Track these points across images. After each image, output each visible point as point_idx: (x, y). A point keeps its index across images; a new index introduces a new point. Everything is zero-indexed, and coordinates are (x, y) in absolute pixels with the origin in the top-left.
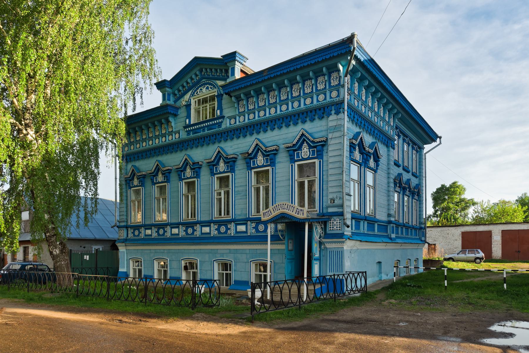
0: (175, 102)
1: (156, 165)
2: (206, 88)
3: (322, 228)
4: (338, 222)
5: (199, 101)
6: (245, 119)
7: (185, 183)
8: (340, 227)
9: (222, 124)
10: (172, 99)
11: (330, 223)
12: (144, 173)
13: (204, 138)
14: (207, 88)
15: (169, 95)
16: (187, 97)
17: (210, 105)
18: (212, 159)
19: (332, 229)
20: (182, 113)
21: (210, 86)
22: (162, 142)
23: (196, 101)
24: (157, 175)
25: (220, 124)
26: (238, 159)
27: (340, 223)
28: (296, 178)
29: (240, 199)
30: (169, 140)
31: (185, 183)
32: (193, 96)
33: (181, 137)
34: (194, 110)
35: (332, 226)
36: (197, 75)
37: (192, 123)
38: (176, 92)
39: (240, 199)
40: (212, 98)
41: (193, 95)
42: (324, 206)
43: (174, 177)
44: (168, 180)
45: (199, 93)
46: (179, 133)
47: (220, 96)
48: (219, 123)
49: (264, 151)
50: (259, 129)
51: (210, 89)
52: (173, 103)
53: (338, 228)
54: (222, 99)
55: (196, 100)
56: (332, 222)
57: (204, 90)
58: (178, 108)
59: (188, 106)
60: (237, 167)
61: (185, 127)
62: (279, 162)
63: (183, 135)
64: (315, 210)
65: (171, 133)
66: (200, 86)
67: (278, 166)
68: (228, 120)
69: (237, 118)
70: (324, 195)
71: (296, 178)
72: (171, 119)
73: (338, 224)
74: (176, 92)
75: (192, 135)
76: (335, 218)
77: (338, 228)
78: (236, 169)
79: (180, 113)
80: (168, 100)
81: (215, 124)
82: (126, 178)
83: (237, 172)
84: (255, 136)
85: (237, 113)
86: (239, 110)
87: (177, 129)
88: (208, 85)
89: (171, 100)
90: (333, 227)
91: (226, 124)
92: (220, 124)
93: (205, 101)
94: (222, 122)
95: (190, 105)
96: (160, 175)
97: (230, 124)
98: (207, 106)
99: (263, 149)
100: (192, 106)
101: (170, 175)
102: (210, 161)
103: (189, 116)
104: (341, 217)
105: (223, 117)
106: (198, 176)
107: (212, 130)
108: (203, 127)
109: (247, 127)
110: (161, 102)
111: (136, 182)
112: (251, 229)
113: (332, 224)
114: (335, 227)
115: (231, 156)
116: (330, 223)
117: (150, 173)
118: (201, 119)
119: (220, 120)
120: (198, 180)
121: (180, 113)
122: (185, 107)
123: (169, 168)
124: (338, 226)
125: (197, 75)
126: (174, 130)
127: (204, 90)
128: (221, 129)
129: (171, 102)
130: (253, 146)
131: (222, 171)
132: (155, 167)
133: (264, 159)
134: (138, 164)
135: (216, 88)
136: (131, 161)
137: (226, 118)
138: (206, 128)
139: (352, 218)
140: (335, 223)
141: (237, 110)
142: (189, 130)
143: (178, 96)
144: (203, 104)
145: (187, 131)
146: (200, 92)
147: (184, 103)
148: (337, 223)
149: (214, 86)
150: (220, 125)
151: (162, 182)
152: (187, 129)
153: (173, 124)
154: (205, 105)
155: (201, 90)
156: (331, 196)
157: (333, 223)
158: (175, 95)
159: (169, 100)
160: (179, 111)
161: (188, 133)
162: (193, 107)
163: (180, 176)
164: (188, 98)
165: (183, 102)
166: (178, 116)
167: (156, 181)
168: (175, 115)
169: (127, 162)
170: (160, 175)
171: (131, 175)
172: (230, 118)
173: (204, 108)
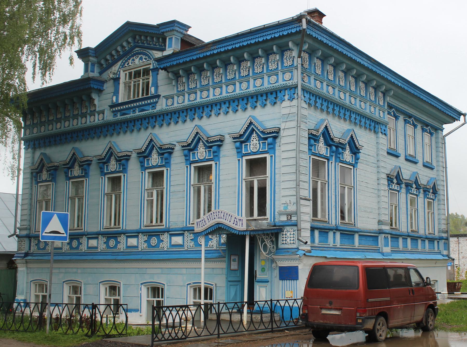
0: (101, 73)
1: (72, 153)
2: (139, 59)
3: (272, 241)
4: (292, 233)
5: (130, 74)
7: (109, 178)
9: (157, 105)
10: (97, 70)
11: (283, 235)
12: (56, 164)
13: (134, 121)
14: (141, 58)
15: (93, 65)
16: (115, 68)
17: (143, 80)
19: (284, 242)
20: (108, 87)
21: (144, 57)
22: (81, 124)
23: (126, 74)
24: (72, 167)
26: (175, 150)
27: (293, 234)
28: (244, 177)
30: (90, 122)
31: (109, 178)
32: (123, 67)
33: (105, 119)
34: (123, 85)
35: (284, 239)
36: (129, 43)
37: (120, 102)
38: (103, 62)
40: (146, 72)
41: (123, 66)
42: (276, 213)
43: (94, 171)
44: (86, 175)
45: (130, 64)
46: (103, 113)
47: (155, 70)
49: (205, 141)
51: (144, 60)
52: (98, 75)
54: (158, 74)
55: (127, 72)
56: (284, 233)
57: (137, 61)
58: (103, 82)
59: (116, 80)
60: (173, 161)
61: (111, 107)
62: (224, 156)
63: (109, 117)
64: (266, 217)
65: (93, 113)
66: (133, 56)
69: (176, 98)
70: (276, 199)
71: (244, 177)
72: (94, 96)
73: (292, 236)
74: (103, 62)
75: (119, 117)
76: (288, 228)
77: (292, 242)
79: (106, 88)
80: (91, 71)
81: (149, 104)
82: (32, 170)
83: (173, 167)
85: (175, 92)
87: (101, 109)
88: (141, 55)
89: (95, 71)
90: (286, 240)
91: (162, 105)
93: (137, 74)
94: (157, 102)
96: (77, 167)
97: (167, 105)
98: (139, 81)
101: (89, 168)
102: (140, 151)
103: (116, 93)
104: (295, 228)
105: (158, 96)
106: (124, 170)
107: (144, 112)
108: (135, 107)
109: (187, 109)
110: (83, 74)
111: (45, 175)
113: (284, 236)
114: (288, 240)
115: (167, 147)
116: (283, 235)
117: (64, 165)
118: (132, 96)
119: (155, 100)
120: (124, 175)
121: (106, 88)
122: (112, 81)
123: (89, 158)
124: (292, 239)
125: (129, 43)
126: (97, 110)
127: (137, 61)
128: (155, 111)
129: (95, 74)
131: (155, 164)
132: (70, 157)
134: (49, 151)
135: (151, 60)
136: (40, 147)
138: (137, 109)
139: (313, 229)
140: (288, 234)
141: (175, 88)
142: (116, 111)
143: (104, 66)
144: (135, 78)
145: (113, 112)
146: (132, 63)
147: (111, 76)
148: (290, 234)
149: (149, 57)
150: (154, 105)
151: (79, 177)
152: (114, 109)
153: (96, 102)
154: (137, 79)
155: (133, 60)
156: (284, 200)
157: (286, 234)
158: (102, 65)
159: (93, 71)
160: (105, 86)
162: (122, 80)
163: (101, 169)
164: (117, 70)
165: (110, 74)
166: (104, 92)
167: (71, 174)
168: (100, 91)
169: (34, 149)
170: (77, 167)
171: (39, 166)
172: (167, 98)
173: (136, 83)
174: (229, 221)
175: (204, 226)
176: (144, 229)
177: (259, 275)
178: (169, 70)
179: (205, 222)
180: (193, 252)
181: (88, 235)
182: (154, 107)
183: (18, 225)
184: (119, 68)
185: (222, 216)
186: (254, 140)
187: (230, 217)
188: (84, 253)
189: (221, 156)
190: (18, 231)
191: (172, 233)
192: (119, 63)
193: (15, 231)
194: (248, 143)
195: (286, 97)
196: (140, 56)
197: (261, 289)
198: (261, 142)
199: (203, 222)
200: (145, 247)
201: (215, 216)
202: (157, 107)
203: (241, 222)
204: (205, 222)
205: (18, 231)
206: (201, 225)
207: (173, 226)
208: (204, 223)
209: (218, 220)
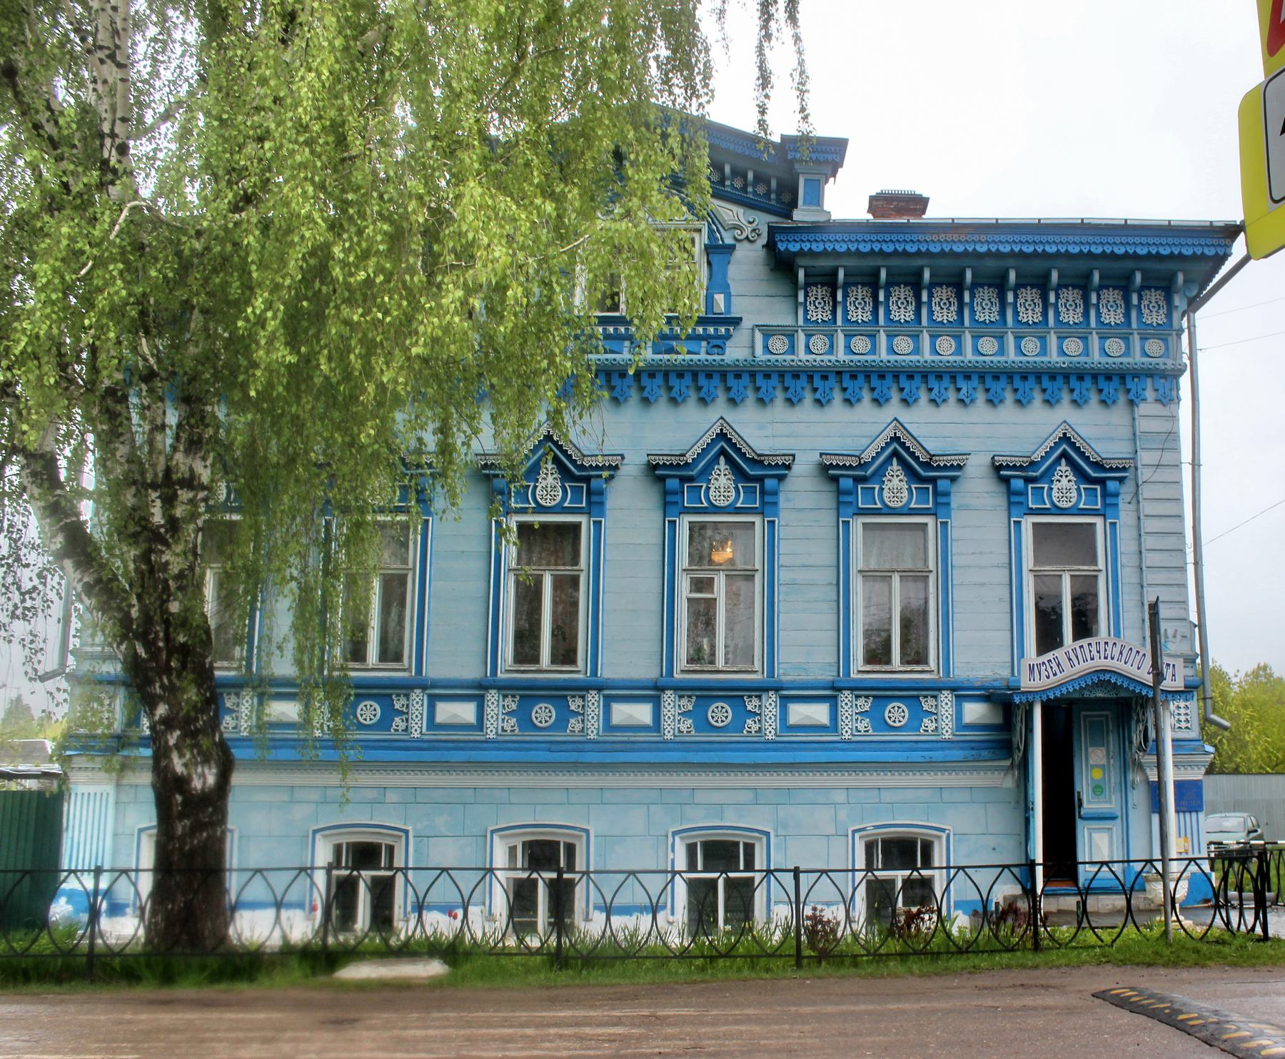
6: (832, 346)
8: (1187, 721)
9: (728, 343)
25: (718, 342)
50: (943, 391)
53: (1183, 725)
60: (788, 500)
62: (960, 508)
67: (958, 520)
68: (759, 337)
69: (801, 337)
73: (1182, 711)
84: (894, 409)
85: (801, 322)
86: (806, 312)
92: (718, 342)
94: (728, 337)
99: (916, 459)
109: (839, 373)
112: (677, 718)
119: (722, 330)
124: (1182, 718)
130: (881, 442)
133: (910, 489)
137: (747, 323)
150: (718, 344)
174: (1135, 665)
175: (1055, 675)
176: (681, 681)
177: (1089, 802)
178: (800, 261)
179: (1059, 665)
180: (873, 745)
181: (434, 686)
182: (721, 348)
183: (74, 642)
185: (1117, 655)
186: (1064, 480)
187: (1138, 658)
188: (418, 740)
189: (953, 505)
190: (71, 660)
191: (788, 694)
193: (63, 663)
194: (1046, 486)
195: (1150, 394)
197: (1095, 836)
198: (1082, 486)
199: (1054, 665)
200: (685, 730)
201: (1094, 652)
202: (727, 350)
203: (1170, 670)
204: (1059, 665)
205: (71, 660)
206: (1044, 673)
208: (1055, 668)
209: (1100, 663)
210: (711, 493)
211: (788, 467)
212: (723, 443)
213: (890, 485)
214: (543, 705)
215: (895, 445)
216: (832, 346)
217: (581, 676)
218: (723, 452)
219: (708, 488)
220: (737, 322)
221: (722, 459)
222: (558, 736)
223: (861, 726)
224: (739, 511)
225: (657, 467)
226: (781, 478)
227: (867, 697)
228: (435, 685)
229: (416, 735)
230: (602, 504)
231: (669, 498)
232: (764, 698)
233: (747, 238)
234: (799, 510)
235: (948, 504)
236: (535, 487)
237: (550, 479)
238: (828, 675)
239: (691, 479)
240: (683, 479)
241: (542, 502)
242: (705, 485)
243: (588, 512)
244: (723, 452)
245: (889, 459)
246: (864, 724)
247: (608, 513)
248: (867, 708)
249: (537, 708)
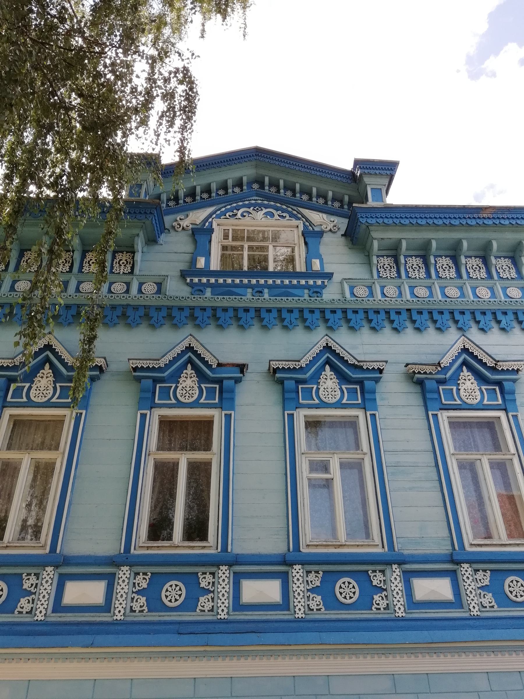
6: (400, 293)
9: (324, 291)
18: (303, 363)
29: (411, 489)
39: (411, 489)
45: (239, 216)
48: (315, 286)
51: (276, 217)
57: (260, 215)
60: (382, 399)
61: (183, 275)
78: (379, 402)
94: (323, 286)
95: (211, 231)
99: (484, 365)
100: (214, 236)
119: (319, 282)
137: (337, 278)
138: (266, 291)
150: (317, 291)
152: (196, 280)
161: (198, 289)
162: (216, 238)
166: (157, 248)
184: (210, 216)
192: (210, 210)
196: (265, 211)
207: (408, 550)
210: (321, 392)
211: (381, 371)
212: (328, 355)
213: (464, 387)
214: (173, 583)
215: (464, 356)
216: (400, 293)
217: (212, 551)
218: (328, 362)
219: (318, 389)
220: (329, 276)
221: (327, 367)
222: (187, 617)
223: (485, 602)
224: (345, 406)
225: (275, 371)
226: (377, 380)
227: (485, 571)
228: (67, 561)
229: (40, 617)
230: (232, 399)
231: (287, 395)
232: (388, 572)
233: (330, 230)
234: (393, 407)
235: (515, 400)
236: (177, 387)
237: (189, 382)
238: (444, 549)
239: (304, 382)
240: (299, 382)
241: (182, 399)
242: (315, 387)
243: (220, 406)
244: (328, 362)
245: (460, 368)
246: (488, 599)
247: (236, 408)
248: (487, 582)
249: (167, 586)
